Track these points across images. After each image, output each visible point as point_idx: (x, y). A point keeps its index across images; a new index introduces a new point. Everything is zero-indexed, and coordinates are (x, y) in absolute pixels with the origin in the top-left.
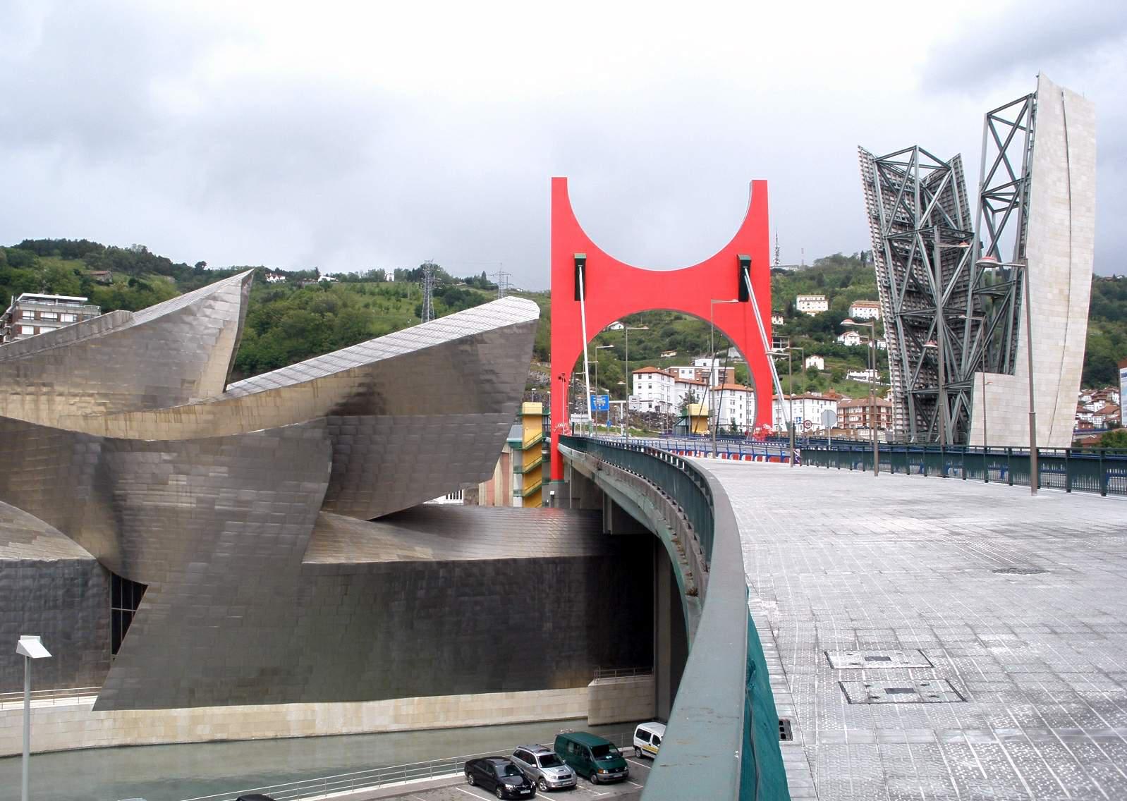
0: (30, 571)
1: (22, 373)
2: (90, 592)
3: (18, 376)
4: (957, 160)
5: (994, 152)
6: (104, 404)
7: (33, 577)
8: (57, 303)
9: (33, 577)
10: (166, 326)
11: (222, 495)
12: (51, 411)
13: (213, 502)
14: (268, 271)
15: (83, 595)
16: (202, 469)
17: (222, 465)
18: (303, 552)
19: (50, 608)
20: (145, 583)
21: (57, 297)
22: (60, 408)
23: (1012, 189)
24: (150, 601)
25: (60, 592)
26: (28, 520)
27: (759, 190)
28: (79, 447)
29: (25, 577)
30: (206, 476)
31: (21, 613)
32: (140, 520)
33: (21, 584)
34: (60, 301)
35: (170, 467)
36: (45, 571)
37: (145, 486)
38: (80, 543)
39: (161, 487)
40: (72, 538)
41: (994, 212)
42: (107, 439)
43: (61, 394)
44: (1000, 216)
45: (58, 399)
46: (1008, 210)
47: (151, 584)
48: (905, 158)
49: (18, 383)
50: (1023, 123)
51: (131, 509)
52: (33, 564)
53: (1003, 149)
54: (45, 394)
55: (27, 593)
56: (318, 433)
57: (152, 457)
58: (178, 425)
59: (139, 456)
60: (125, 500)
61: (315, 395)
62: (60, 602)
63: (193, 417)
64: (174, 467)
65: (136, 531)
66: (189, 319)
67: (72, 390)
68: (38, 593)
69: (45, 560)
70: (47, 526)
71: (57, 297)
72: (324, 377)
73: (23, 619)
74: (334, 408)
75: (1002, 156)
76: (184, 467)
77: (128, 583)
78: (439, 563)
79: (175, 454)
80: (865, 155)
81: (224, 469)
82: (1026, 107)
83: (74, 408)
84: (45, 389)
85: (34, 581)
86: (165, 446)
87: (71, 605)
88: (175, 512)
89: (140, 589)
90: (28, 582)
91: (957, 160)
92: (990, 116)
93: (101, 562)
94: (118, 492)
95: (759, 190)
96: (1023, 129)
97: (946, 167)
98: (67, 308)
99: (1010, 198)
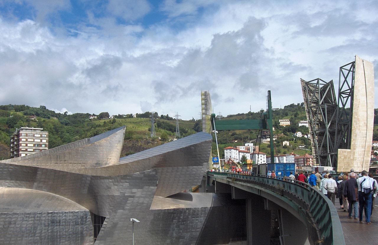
0: (71, 214)
1: (58, 157)
2: (88, 220)
4: (331, 82)
5: (343, 79)
8: (33, 131)
14: (90, 115)
15: (86, 221)
17: (127, 182)
18: (149, 206)
19: (76, 225)
21: (33, 128)
22: (70, 167)
23: (349, 91)
24: (106, 222)
25: (80, 220)
27: (269, 92)
29: (70, 216)
32: (103, 199)
33: (69, 218)
34: (34, 130)
36: (75, 214)
37: (104, 189)
39: (109, 189)
41: (344, 98)
42: (92, 176)
43: (71, 163)
44: (345, 99)
46: (348, 97)
47: (107, 217)
48: (316, 82)
50: (352, 70)
53: (346, 78)
55: (70, 221)
59: (103, 181)
64: (113, 184)
65: (101, 202)
67: (75, 162)
68: (73, 221)
71: (33, 128)
74: (155, 165)
75: (346, 80)
76: (117, 183)
77: (99, 217)
78: (186, 209)
79: (113, 180)
80: (302, 81)
82: (352, 66)
83: (75, 167)
87: (82, 224)
88: (113, 196)
89: (103, 219)
90: (71, 217)
91: (331, 82)
92: (341, 68)
94: (96, 191)
95: (269, 92)
96: (351, 71)
97: (328, 84)
98: (37, 132)
99: (348, 93)
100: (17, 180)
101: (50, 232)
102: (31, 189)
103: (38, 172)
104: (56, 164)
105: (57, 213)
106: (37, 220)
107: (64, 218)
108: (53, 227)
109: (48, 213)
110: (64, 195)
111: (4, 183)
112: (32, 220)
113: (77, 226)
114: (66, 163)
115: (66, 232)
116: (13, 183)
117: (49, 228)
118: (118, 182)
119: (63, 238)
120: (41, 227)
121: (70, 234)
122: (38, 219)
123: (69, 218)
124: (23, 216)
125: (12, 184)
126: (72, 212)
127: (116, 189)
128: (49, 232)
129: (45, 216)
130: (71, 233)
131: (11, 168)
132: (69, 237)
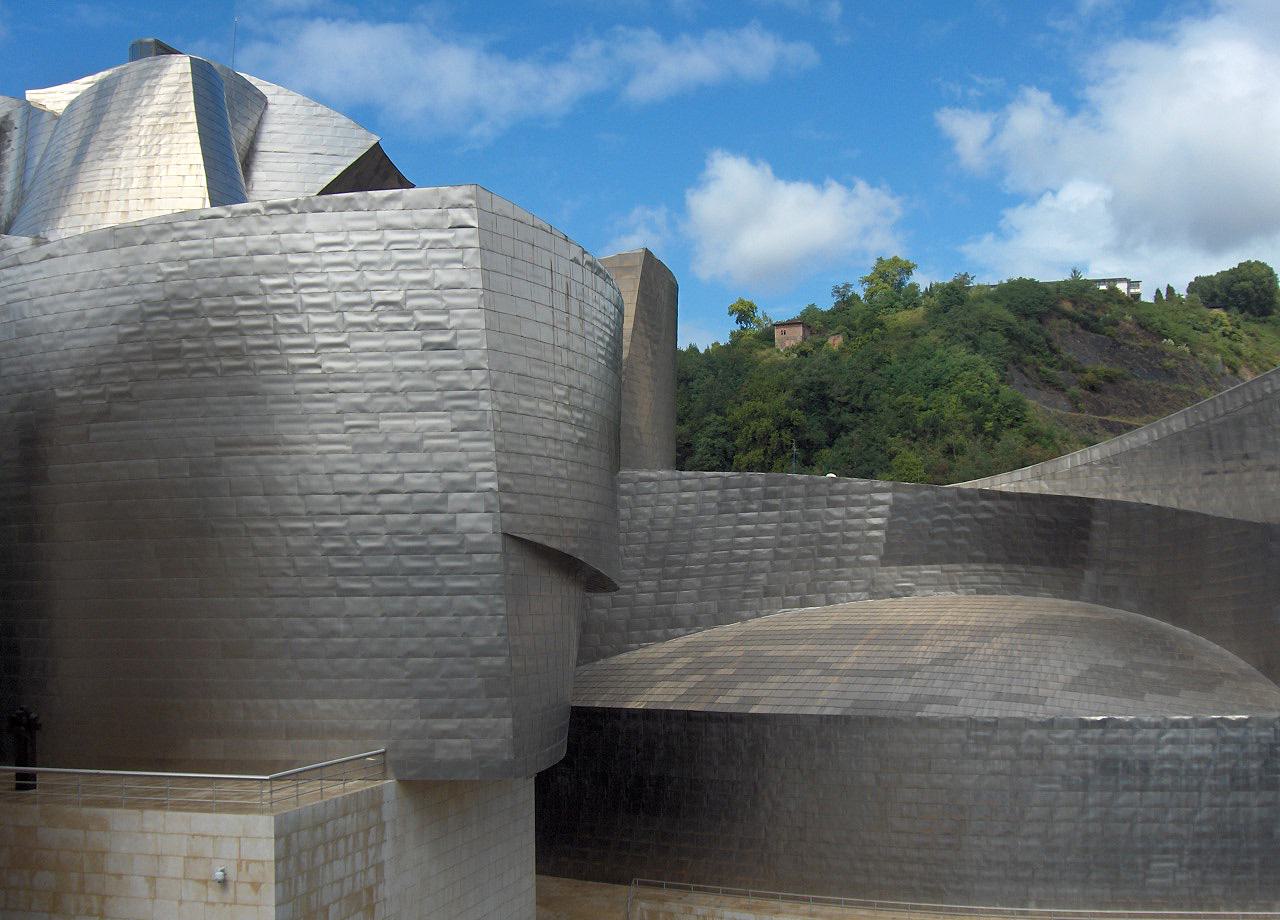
0: (1209, 734)
7: (1213, 743)
9: (1213, 743)
19: (1238, 789)
25: (1254, 765)
31: (1196, 794)
62: (1254, 779)
70: (1243, 664)
73: (1200, 803)
85: (1214, 749)
90: (1206, 750)
100: (1012, 560)
101: (1094, 820)
102: (1071, 599)
103: (1094, 523)
104: (1210, 478)
105: (1129, 725)
106: (1030, 757)
107: (1167, 750)
108: (1108, 794)
109: (1085, 725)
110: (1198, 627)
111: (960, 576)
112: (1003, 758)
113: (1241, 796)
114: (1249, 470)
115: (1177, 821)
116: (997, 573)
117: (1091, 800)
119: (1165, 851)
120: (1050, 790)
121: (1200, 836)
122: (1035, 750)
124: (963, 736)
125: (997, 579)
126: (1212, 724)
128: (1091, 815)
129: (1066, 741)
130: (1205, 829)
131: (986, 509)
132: (1198, 852)
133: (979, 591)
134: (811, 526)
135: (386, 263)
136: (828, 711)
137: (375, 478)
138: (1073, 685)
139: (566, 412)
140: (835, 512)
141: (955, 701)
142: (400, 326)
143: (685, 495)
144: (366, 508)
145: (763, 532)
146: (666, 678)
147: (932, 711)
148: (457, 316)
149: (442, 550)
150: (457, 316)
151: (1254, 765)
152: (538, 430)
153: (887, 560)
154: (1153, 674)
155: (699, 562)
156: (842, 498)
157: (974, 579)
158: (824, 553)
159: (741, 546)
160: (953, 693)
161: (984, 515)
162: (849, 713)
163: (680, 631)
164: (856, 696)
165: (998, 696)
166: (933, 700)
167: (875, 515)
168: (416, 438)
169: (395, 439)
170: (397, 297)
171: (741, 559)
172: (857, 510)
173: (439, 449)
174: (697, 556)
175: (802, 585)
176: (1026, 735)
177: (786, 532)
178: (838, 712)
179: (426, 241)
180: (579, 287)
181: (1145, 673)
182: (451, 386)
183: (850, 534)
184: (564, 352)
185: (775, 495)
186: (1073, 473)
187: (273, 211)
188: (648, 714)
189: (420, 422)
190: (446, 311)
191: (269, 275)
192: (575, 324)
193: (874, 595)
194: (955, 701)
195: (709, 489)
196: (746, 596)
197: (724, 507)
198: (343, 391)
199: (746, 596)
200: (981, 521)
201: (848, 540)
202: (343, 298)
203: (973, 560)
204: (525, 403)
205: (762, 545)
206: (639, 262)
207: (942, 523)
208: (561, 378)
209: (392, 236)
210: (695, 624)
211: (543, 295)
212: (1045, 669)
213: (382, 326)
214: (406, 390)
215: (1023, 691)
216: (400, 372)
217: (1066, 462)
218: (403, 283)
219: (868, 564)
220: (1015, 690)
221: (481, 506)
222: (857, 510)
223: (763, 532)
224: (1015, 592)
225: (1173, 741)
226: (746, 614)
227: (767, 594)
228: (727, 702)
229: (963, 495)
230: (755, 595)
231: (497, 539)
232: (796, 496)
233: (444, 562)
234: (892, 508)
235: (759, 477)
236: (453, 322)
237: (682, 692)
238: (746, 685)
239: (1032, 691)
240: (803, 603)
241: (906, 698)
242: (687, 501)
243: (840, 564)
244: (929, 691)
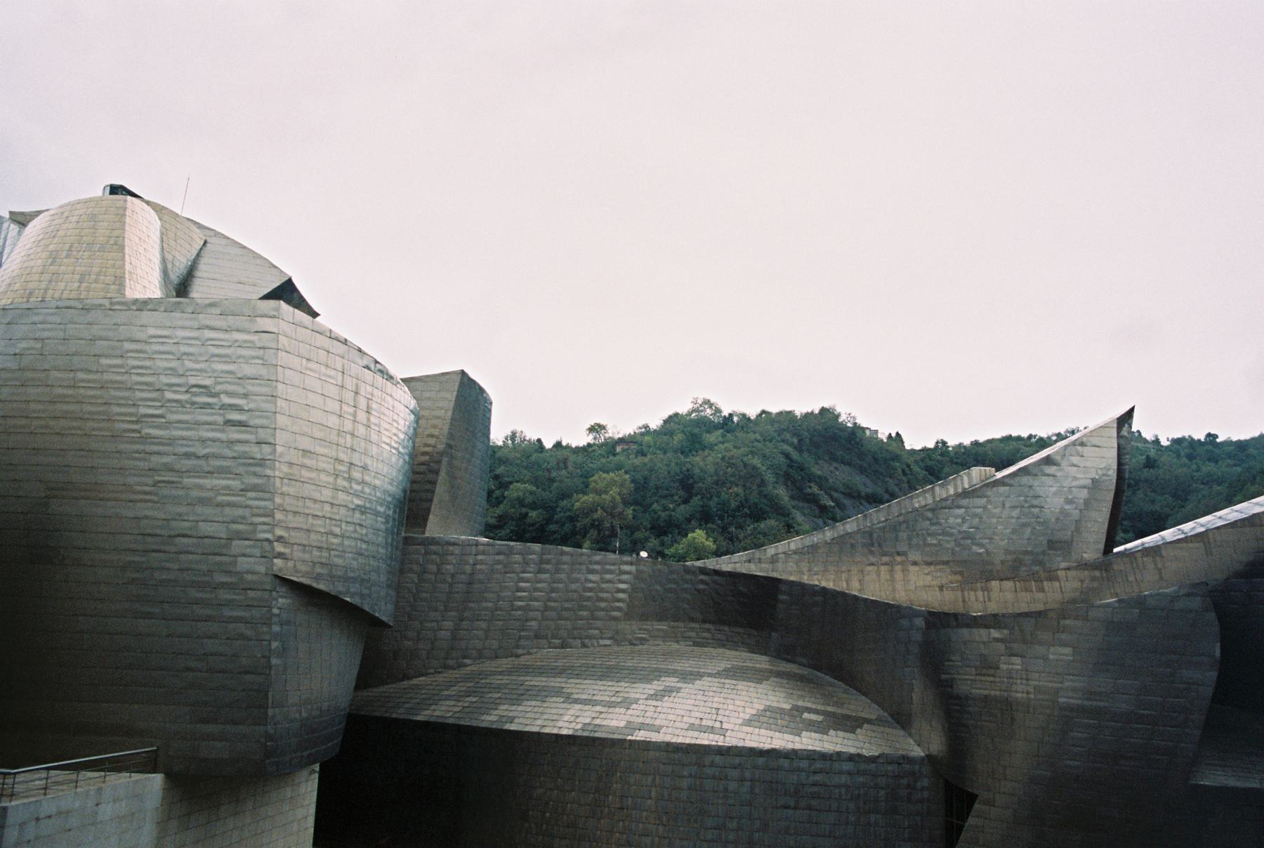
0: (847, 766)
3: (872, 545)
6: (961, 573)
9: (849, 773)
10: (1025, 480)
11: (1067, 684)
12: (906, 581)
13: (1057, 691)
16: (1040, 650)
17: (1064, 645)
20: (976, 792)
25: (882, 793)
26: (860, 706)
28: (905, 623)
30: (1046, 659)
32: (969, 713)
35: (1001, 647)
38: (910, 735)
39: (992, 672)
40: (903, 728)
43: (915, 563)
45: (913, 569)
49: (872, 553)
51: (958, 697)
52: (852, 758)
54: (886, 564)
55: (843, 790)
56: (1196, 603)
57: (981, 634)
58: (1040, 595)
59: (965, 631)
60: (951, 687)
61: (1208, 552)
63: (1056, 584)
66: (1051, 470)
68: (856, 792)
69: (865, 753)
72: (1218, 528)
79: (1006, 631)
81: (1068, 650)
84: (899, 559)
86: (994, 621)
89: (972, 798)
93: (930, 758)
94: (943, 677)
100: (720, 621)
107: (818, 778)
116: (708, 630)
118: (1025, 642)
123: (836, 780)
127: (1017, 671)
131: (702, 582)
133: (696, 644)
134: (573, 586)
135: (201, 355)
136: (564, 732)
137: (173, 524)
138: (748, 723)
139: (346, 484)
140: (591, 577)
141: (658, 730)
142: (209, 406)
143: (480, 557)
144: (167, 548)
145: (536, 590)
146: (448, 698)
147: (640, 736)
148: (255, 401)
149: (223, 585)
150: (255, 401)
151: (882, 793)
152: (317, 496)
153: (628, 616)
154: (813, 717)
155: (486, 609)
156: (597, 567)
157: (693, 634)
158: (582, 608)
159: (520, 599)
160: (657, 722)
161: (701, 587)
162: (579, 734)
163: (468, 661)
164: (588, 721)
165: (692, 727)
166: (642, 727)
167: (621, 582)
168: (210, 494)
169: (195, 493)
170: (207, 382)
171: (520, 608)
172: (608, 576)
173: (229, 504)
174: (484, 604)
175: (563, 633)
176: (707, 760)
177: (553, 590)
178: (570, 732)
179: (236, 341)
180: (369, 389)
181: (806, 715)
182: (245, 455)
183: (601, 595)
184: (349, 437)
185: (548, 562)
186: (774, 560)
187: (117, 307)
188: (426, 724)
189: (216, 482)
190: (245, 396)
191: (107, 356)
192: (362, 416)
193: (618, 643)
194: (658, 730)
195: (498, 554)
196: (520, 637)
197: (508, 568)
198: (159, 453)
199: (520, 637)
200: (699, 591)
201: (602, 600)
202: (165, 380)
203: (692, 620)
204: (305, 473)
205: (536, 600)
206: (458, 378)
207: (671, 590)
208: (342, 456)
209: (209, 334)
210: (480, 656)
211: (333, 391)
212: (731, 707)
213: (193, 403)
214: (206, 457)
215: (710, 723)
216: (203, 441)
217: (771, 550)
218: (214, 371)
219: (615, 619)
220: (704, 723)
221: (257, 552)
222: (608, 576)
223: (536, 590)
224: (723, 646)
225: (820, 771)
226: (520, 651)
227: (537, 637)
228: (489, 719)
229: (688, 570)
230: (528, 638)
231: (268, 579)
232: (565, 563)
233: (224, 595)
234: (636, 577)
235: (537, 547)
236: (252, 406)
237: (458, 709)
238: (505, 707)
239: (718, 725)
240: (563, 646)
241: (622, 724)
242: (482, 562)
243: (594, 618)
244: (640, 720)
